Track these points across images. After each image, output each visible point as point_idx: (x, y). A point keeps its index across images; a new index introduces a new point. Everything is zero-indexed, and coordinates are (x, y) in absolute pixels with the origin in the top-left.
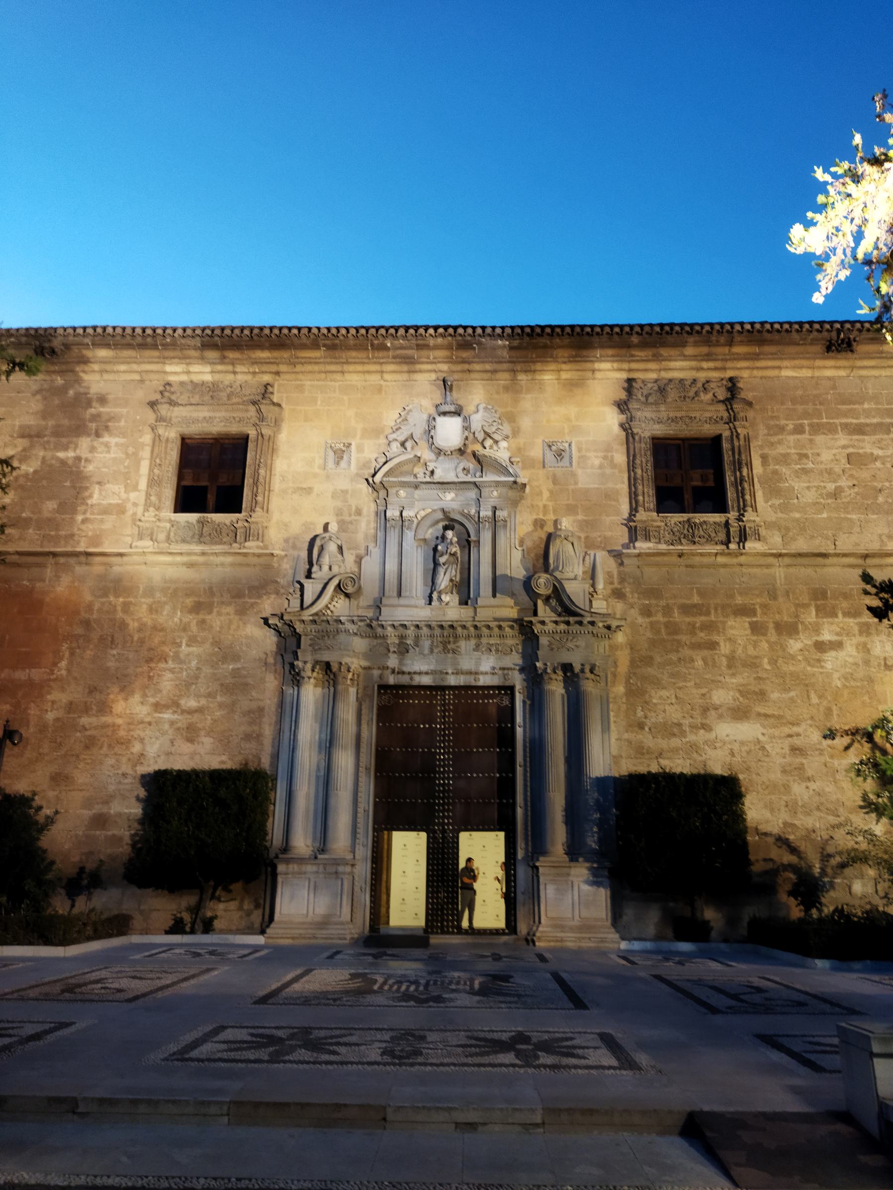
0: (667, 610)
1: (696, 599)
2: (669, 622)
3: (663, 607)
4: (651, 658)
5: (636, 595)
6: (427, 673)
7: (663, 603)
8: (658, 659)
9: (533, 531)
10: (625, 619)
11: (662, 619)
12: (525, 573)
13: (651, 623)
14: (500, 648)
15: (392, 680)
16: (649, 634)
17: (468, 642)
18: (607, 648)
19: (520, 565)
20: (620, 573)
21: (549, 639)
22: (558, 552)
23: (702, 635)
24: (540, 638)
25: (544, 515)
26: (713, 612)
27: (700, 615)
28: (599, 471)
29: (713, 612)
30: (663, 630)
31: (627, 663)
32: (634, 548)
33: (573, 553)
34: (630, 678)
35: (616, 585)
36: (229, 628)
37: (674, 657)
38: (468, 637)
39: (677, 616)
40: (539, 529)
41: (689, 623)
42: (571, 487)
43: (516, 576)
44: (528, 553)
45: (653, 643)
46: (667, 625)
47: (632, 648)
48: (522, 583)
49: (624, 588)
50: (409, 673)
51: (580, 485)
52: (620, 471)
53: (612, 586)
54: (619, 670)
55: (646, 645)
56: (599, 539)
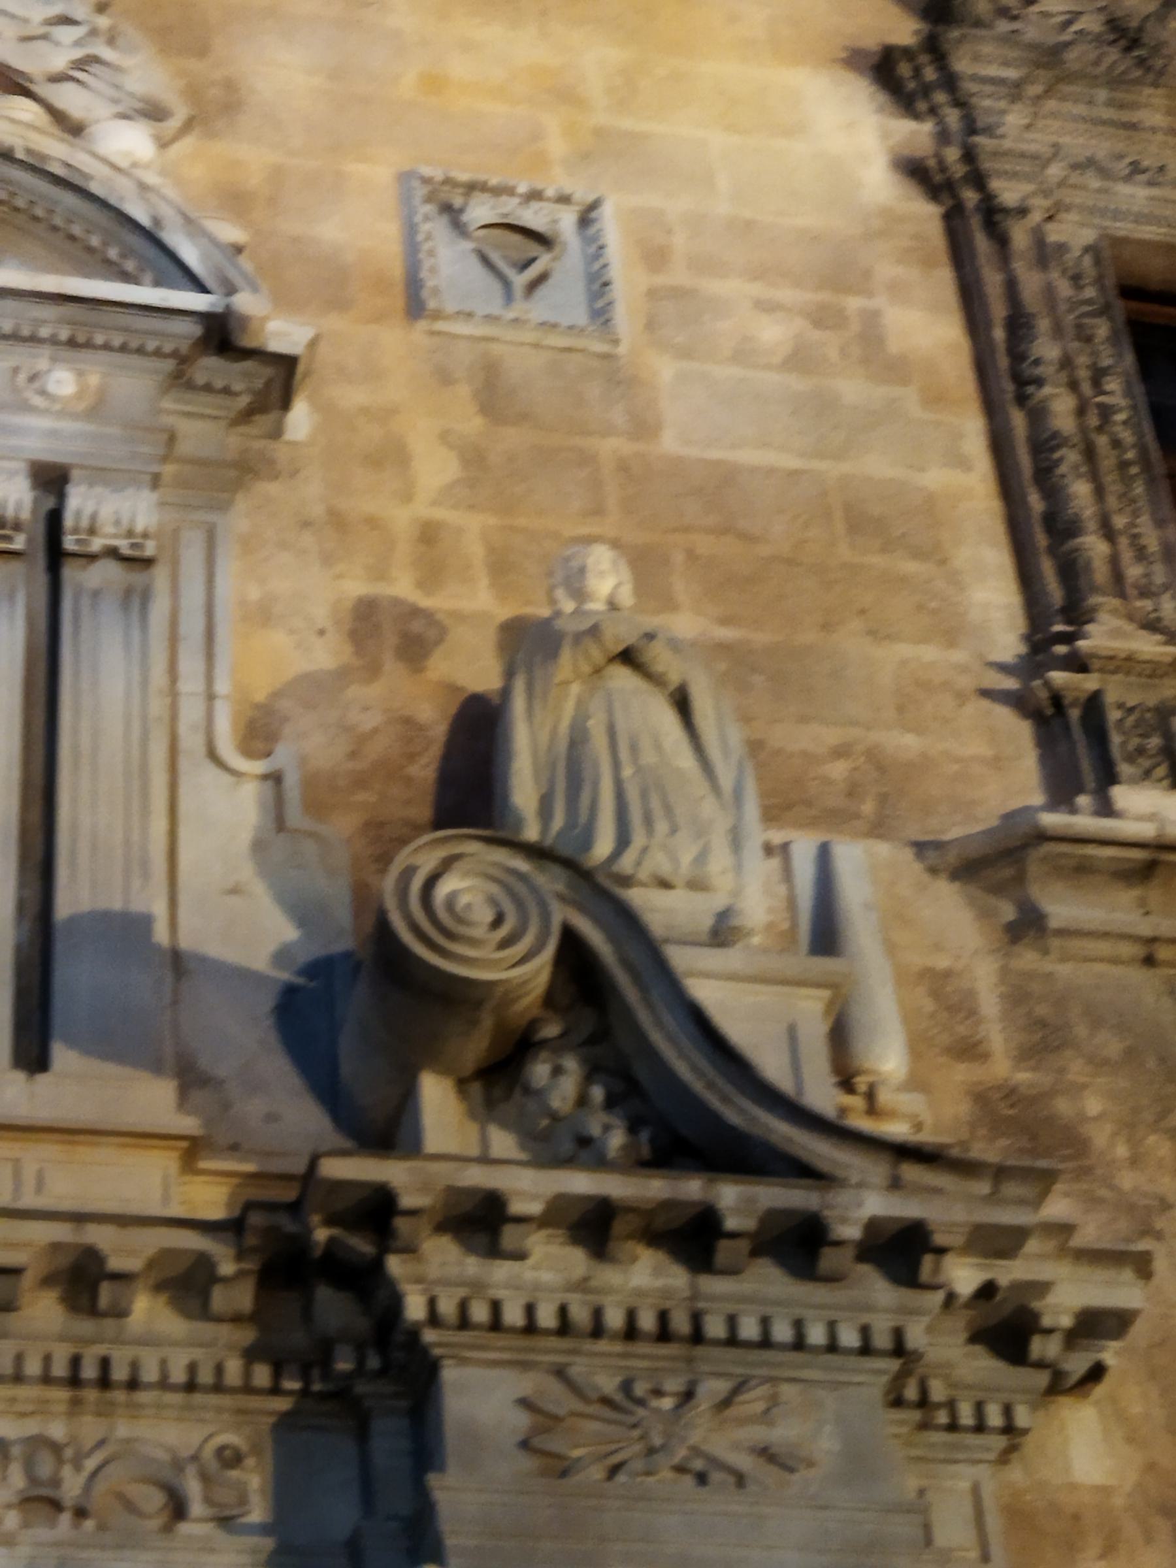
9: (343, 675)
10: (1142, 1266)
12: (290, 933)
14: (72, 1486)
18: (994, 1523)
19: (246, 872)
21: (525, 1384)
22: (578, 740)
24: (450, 1374)
25: (430, 578)
28: (797, 383)
32: (1106, 809)
33: (686, 760)
40: (392, 667)
42: (610, 447)
43: (215, 949)
44: (316, 806)
48: (266, 1002)
51: (669, 443)
52: (935, 398)
53: (963, 1073)
56: (838, 770)
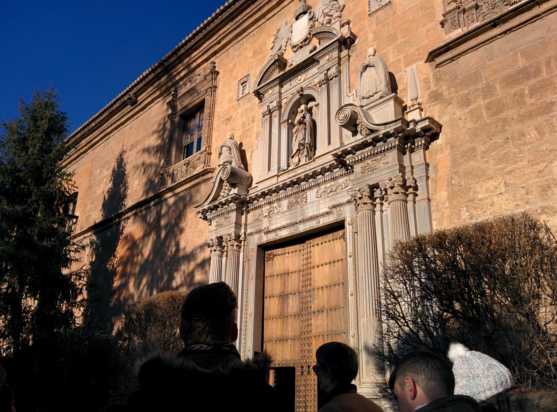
0: (488, 91)
1: (522, 63)
2: (491, 103)
3: (483, 88)
4: (474, 149)
5: (453, 89)
6: (284, 227)
7: (481, 85)
8: (481, 148)
11: (482, 103)
13: (471, 112)
15: (265, 239)
16: (470, 125)
17: (312, 191)
20: (435, 76)
23: (533, 100)
26: (544, 68)
27: (528, 78)
29: (544, 68)
30: (484, 114)
31: (449, 163)
34: (452, 179)
35: (433, 88)
36: (192, 228)
37: (500, 140)
38: (310, 188)
39: (500, 92)
41: (515, 94)
45: (474, 133)
46: (488, 108)
47: (452, 147)
49: (441, 87)
50: (274, 231)
54: (440, 174)
55: (467, 138)
